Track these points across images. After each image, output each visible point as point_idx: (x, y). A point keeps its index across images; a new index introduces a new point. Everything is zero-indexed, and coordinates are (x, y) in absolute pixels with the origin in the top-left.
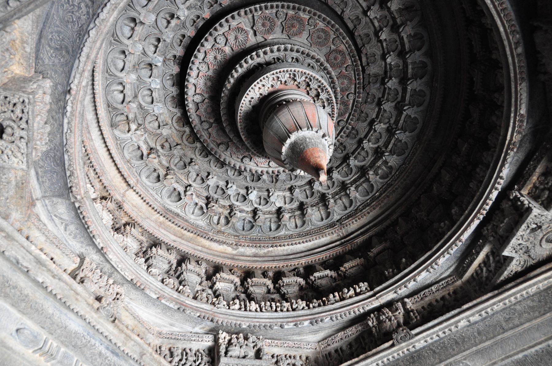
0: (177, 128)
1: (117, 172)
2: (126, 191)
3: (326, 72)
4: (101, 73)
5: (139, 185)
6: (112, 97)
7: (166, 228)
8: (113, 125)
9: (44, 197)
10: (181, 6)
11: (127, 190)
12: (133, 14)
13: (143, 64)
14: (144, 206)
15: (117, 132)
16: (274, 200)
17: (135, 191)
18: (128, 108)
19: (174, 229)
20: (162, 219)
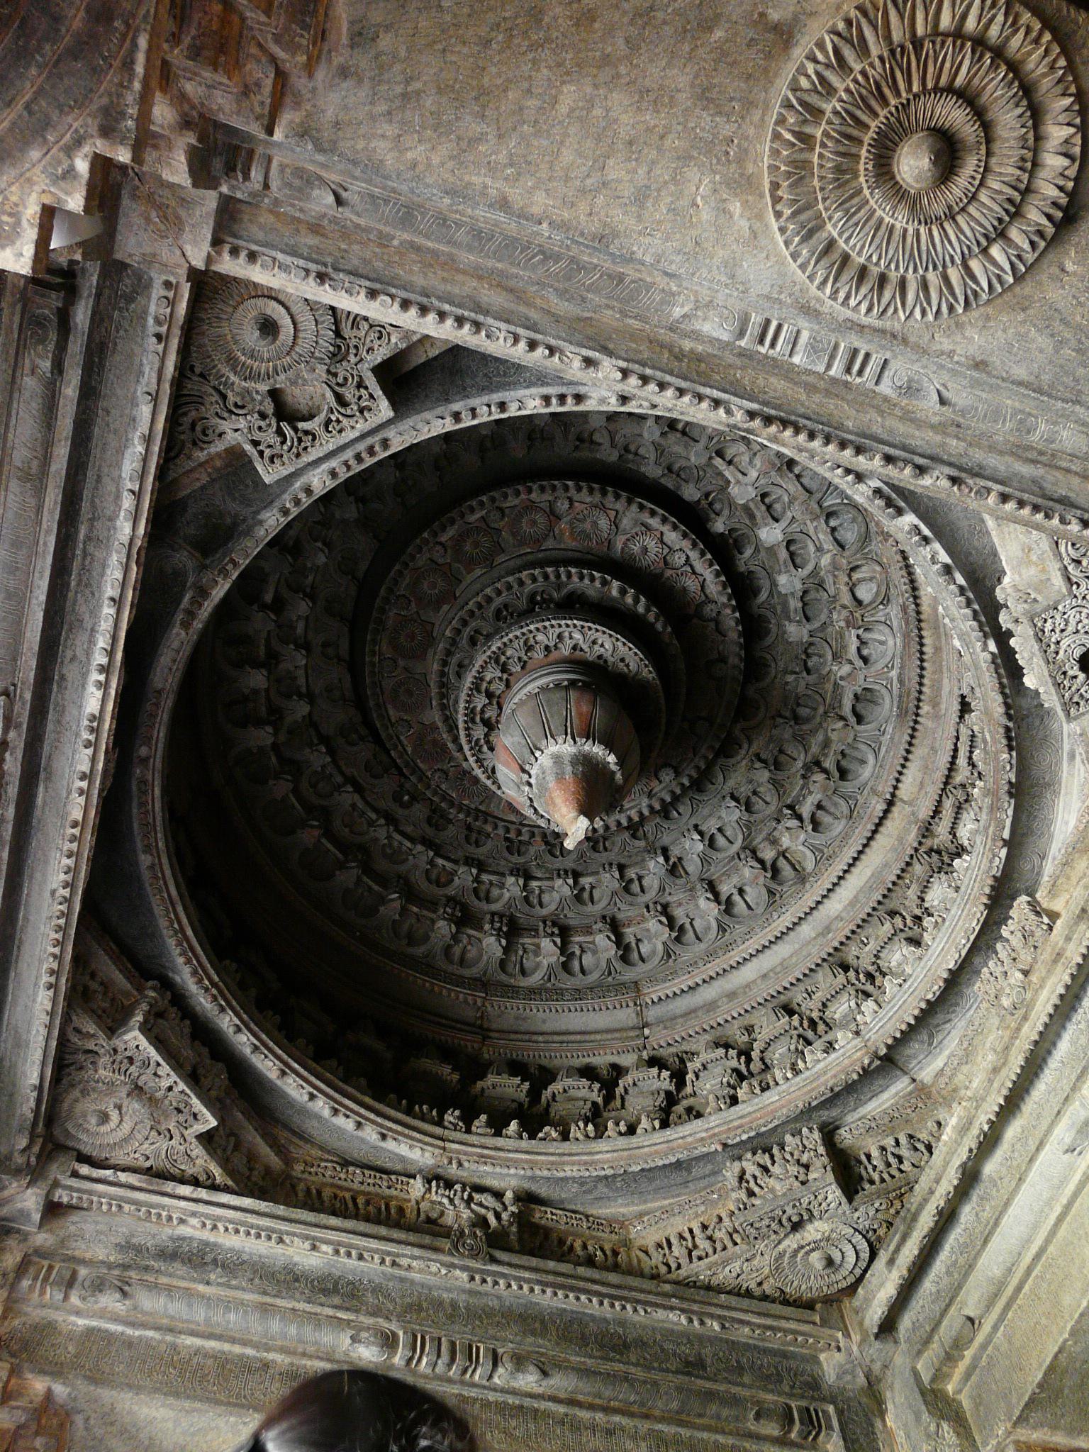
0: (746, 746)
1: (878, 836)
2: (904, 802)
3: (445, 680)
4: (728, 955)
5: (880, 789)
6: (757, 904)
7: (937, 688)
8: (802, 877)
9: (906, 1073)
10: (556, 896)
11: (902, 800)
12: (618, 965)
13: (678, 881)
14: (919, 752)
15: (809, 865)
16: (750, 489)
17: (895, 788)
18: (756, 878)
19: (934, 672)
20: (925, 709)
